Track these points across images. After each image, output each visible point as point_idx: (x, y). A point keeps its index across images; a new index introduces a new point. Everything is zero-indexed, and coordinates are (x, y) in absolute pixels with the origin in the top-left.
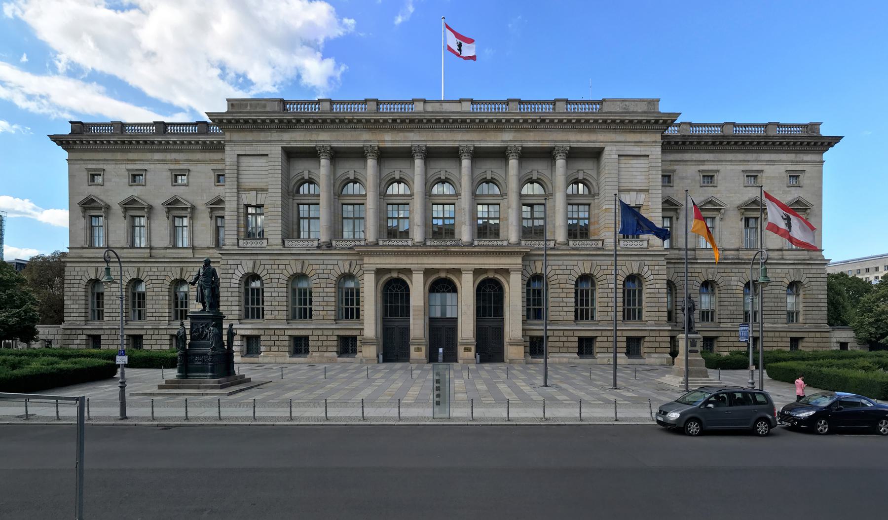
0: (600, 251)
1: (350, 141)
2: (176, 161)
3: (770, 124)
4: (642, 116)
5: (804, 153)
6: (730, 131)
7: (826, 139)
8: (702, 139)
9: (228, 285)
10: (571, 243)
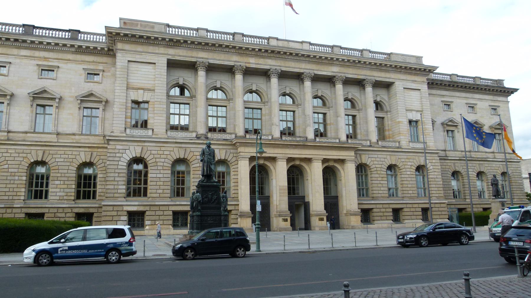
0: (399, 150)
1: (224, 60)
2: (46, 59)
3: (476, 77)
4: (417, 66)
5: (498, 96)
6: (456, 79)
7: (510, 90)
8: (443, 82)
9: (116, 167)
10: (380, 143)
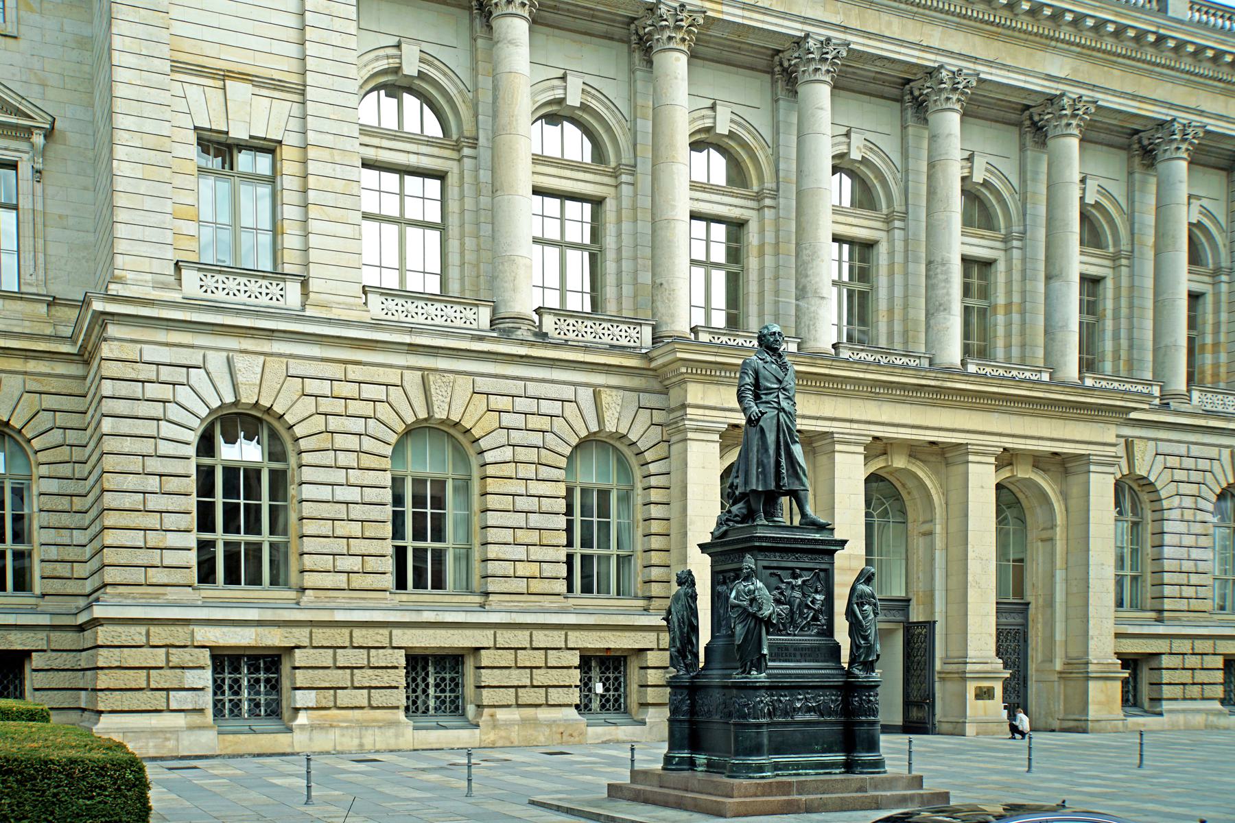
9: (147, 446)
